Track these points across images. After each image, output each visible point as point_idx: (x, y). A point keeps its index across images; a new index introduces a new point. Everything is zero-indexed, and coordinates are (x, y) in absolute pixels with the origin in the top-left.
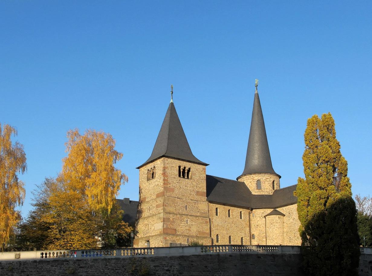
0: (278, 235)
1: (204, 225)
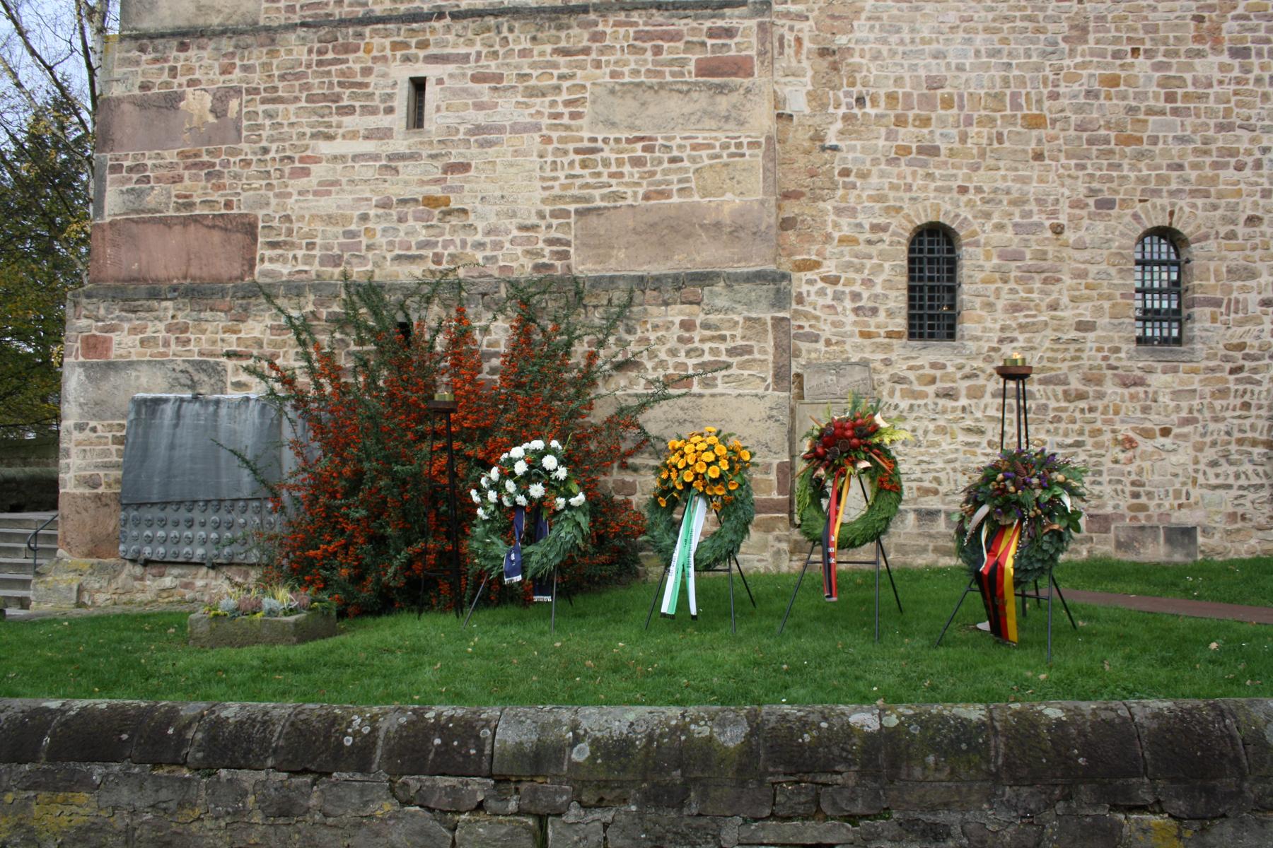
1: (674, 105)
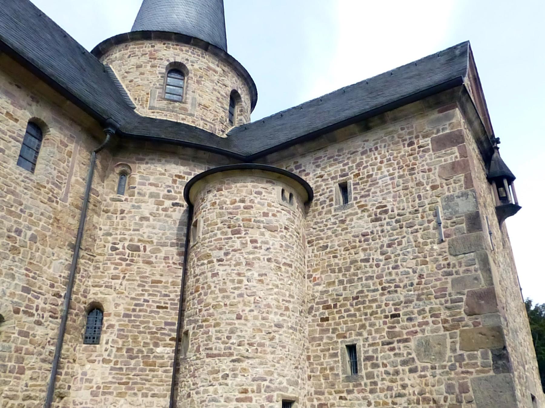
0: (274, 318)
